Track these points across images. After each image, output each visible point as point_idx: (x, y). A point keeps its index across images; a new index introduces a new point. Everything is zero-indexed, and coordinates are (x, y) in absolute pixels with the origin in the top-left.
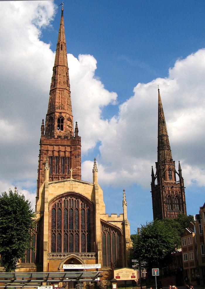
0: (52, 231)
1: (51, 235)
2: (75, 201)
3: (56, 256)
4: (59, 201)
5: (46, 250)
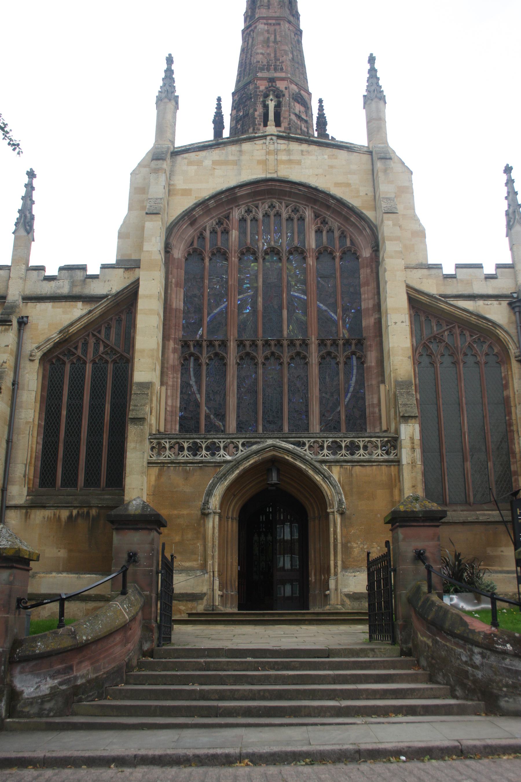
1: (177, 363)
2: (290, 219)
3: (189, 449)
4: (220, 223)
5: (140, 420)
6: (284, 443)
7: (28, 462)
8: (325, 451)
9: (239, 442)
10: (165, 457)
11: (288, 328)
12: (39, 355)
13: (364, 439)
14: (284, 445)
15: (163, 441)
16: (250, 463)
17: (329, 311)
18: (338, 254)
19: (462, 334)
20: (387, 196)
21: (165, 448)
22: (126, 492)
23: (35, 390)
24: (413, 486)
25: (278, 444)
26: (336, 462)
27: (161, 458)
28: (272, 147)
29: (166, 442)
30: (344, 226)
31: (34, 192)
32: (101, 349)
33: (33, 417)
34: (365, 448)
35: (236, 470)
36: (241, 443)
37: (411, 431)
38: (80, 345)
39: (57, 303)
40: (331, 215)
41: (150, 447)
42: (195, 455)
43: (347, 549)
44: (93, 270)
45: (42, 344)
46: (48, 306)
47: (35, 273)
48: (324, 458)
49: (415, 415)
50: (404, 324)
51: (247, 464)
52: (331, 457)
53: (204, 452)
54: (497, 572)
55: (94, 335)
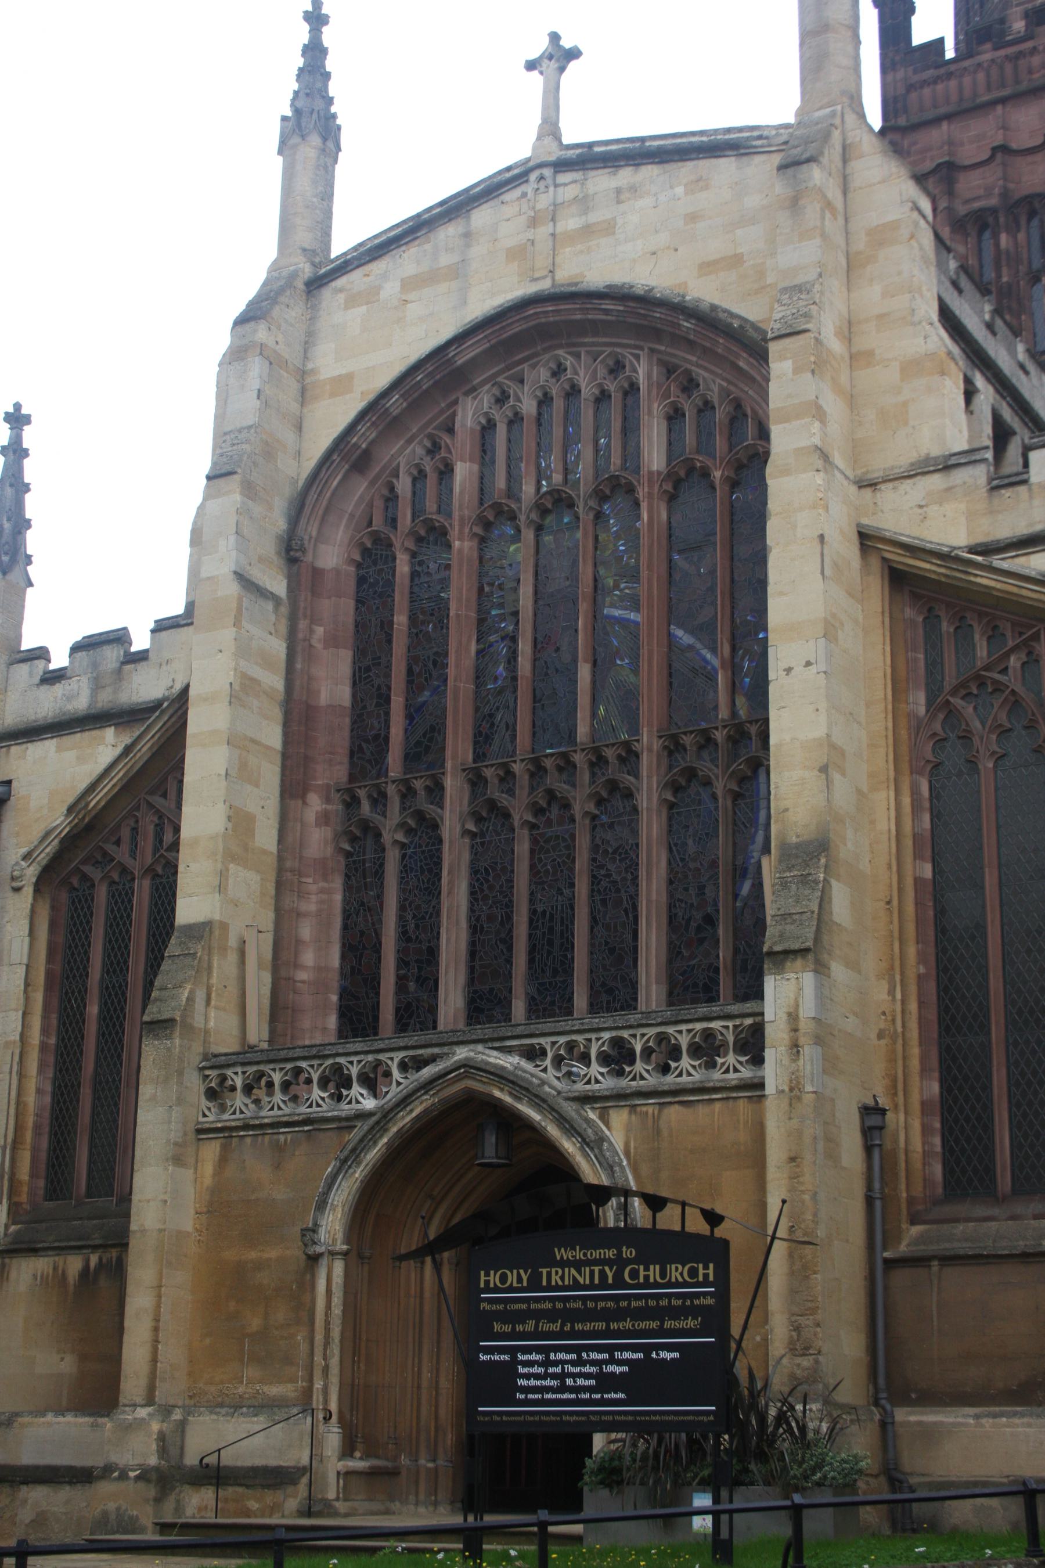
0: (352, 803)
2: (602, 397)
4: (434, 449)
5: (162, 1026)
6: (495, 1053)
7: (10, 1140)
8: (596, 1069)
9: (392, 1059)
10: (234, 1113)
11: (594, 714)
12: (31, 872)
13: (690, 1026)
15: (229, 1072)
16: (414, 1114)
17: (698, 646)
18: (717, 474)
20: (797, 282)
21: (233, 1089)
22: (134, 1210)
23: (25, 961)
24: (792, 1159)
25: (480, 1057)
26: (620, 1097)
27: (226, 1117)
28: (544, 201)
29: (236, 1073)
30: (736, 386)
31: (26, 462)
33: (20, 1029)
34: (695, 1051)
35: (381, 1137)
36: (396, 1061)
37: (792, 996)
38: (125, 833)
39: (65, 738)
40: (701, 362)
41: (202, 1089)
44: (141, 641)
45: (36, 847)
46: (46, 749)
47: (24, 668)
48: (588, 1087)
49: (803, 946)
50: (813, 669)
51: (405, 1119)
52: (609, 1084)
53: (317, 1093)
55: (151, 806)
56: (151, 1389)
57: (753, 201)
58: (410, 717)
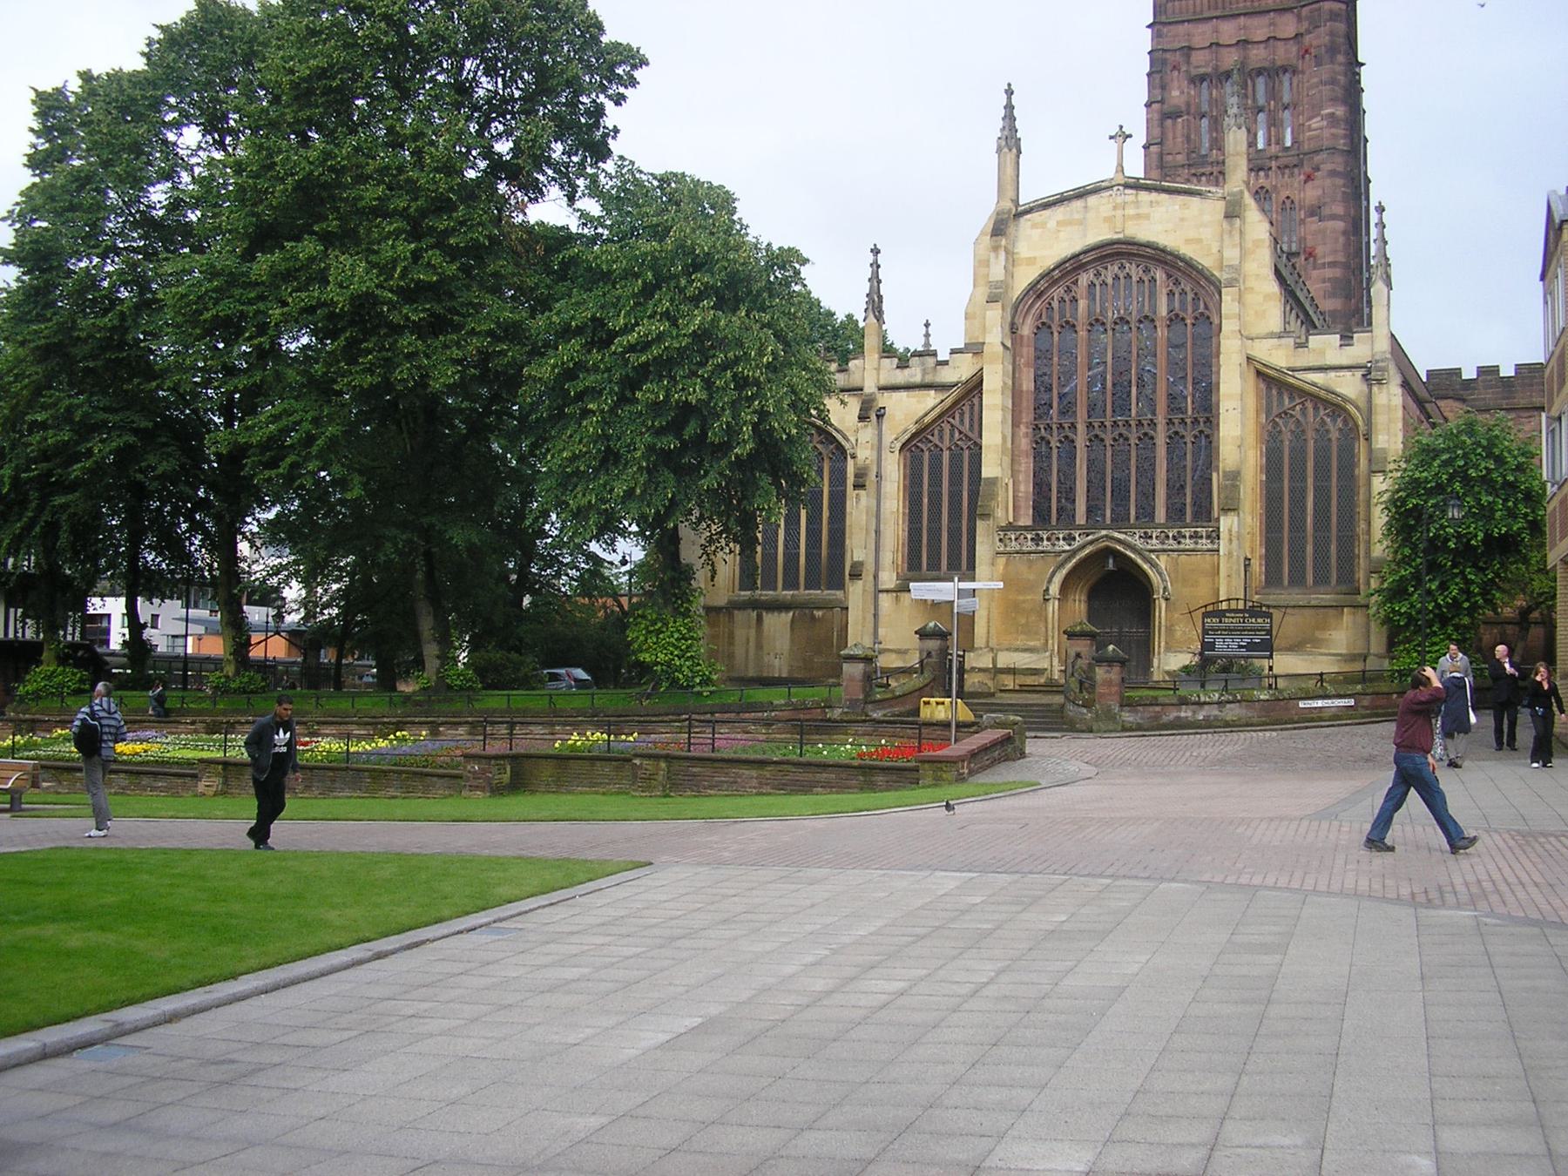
0: (1036, 428)
2: (1141, 281)
4: (1069, 290)
12: (898, 445)
14: (1116, 535)
19: (1316, 408)
26: (1164, 551)
28: (1119, 200)
32: (957, 434)
38: (936, 432)
42: (1038, 545)
43: (1170, 630)
44: (943, 355)
46: (903, 394)
52: (1159, 547)
53: (1045, 542)
54: (1322, 654)
56: (988, 642)
57: (1207, 218)
58: (1060, 398)
